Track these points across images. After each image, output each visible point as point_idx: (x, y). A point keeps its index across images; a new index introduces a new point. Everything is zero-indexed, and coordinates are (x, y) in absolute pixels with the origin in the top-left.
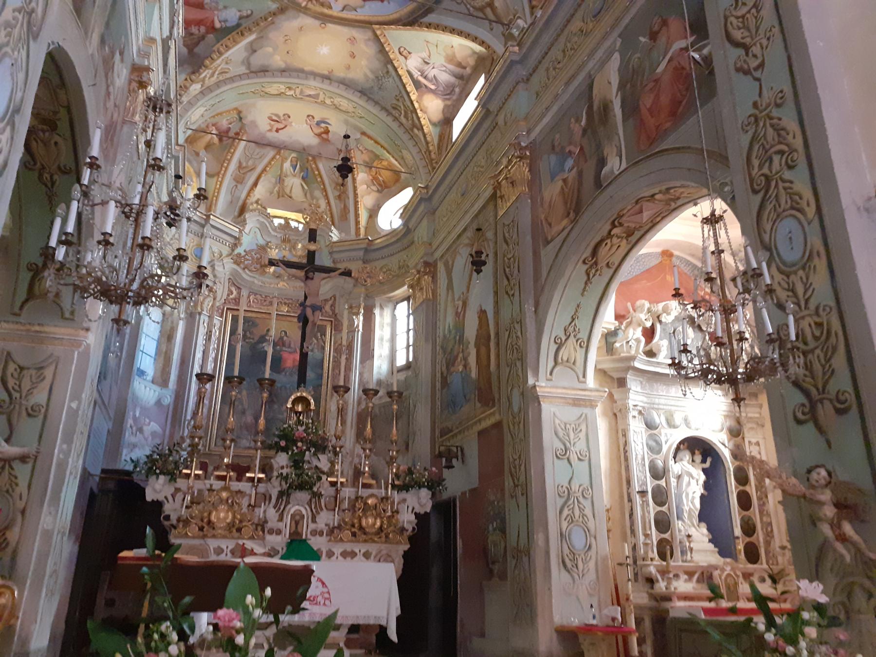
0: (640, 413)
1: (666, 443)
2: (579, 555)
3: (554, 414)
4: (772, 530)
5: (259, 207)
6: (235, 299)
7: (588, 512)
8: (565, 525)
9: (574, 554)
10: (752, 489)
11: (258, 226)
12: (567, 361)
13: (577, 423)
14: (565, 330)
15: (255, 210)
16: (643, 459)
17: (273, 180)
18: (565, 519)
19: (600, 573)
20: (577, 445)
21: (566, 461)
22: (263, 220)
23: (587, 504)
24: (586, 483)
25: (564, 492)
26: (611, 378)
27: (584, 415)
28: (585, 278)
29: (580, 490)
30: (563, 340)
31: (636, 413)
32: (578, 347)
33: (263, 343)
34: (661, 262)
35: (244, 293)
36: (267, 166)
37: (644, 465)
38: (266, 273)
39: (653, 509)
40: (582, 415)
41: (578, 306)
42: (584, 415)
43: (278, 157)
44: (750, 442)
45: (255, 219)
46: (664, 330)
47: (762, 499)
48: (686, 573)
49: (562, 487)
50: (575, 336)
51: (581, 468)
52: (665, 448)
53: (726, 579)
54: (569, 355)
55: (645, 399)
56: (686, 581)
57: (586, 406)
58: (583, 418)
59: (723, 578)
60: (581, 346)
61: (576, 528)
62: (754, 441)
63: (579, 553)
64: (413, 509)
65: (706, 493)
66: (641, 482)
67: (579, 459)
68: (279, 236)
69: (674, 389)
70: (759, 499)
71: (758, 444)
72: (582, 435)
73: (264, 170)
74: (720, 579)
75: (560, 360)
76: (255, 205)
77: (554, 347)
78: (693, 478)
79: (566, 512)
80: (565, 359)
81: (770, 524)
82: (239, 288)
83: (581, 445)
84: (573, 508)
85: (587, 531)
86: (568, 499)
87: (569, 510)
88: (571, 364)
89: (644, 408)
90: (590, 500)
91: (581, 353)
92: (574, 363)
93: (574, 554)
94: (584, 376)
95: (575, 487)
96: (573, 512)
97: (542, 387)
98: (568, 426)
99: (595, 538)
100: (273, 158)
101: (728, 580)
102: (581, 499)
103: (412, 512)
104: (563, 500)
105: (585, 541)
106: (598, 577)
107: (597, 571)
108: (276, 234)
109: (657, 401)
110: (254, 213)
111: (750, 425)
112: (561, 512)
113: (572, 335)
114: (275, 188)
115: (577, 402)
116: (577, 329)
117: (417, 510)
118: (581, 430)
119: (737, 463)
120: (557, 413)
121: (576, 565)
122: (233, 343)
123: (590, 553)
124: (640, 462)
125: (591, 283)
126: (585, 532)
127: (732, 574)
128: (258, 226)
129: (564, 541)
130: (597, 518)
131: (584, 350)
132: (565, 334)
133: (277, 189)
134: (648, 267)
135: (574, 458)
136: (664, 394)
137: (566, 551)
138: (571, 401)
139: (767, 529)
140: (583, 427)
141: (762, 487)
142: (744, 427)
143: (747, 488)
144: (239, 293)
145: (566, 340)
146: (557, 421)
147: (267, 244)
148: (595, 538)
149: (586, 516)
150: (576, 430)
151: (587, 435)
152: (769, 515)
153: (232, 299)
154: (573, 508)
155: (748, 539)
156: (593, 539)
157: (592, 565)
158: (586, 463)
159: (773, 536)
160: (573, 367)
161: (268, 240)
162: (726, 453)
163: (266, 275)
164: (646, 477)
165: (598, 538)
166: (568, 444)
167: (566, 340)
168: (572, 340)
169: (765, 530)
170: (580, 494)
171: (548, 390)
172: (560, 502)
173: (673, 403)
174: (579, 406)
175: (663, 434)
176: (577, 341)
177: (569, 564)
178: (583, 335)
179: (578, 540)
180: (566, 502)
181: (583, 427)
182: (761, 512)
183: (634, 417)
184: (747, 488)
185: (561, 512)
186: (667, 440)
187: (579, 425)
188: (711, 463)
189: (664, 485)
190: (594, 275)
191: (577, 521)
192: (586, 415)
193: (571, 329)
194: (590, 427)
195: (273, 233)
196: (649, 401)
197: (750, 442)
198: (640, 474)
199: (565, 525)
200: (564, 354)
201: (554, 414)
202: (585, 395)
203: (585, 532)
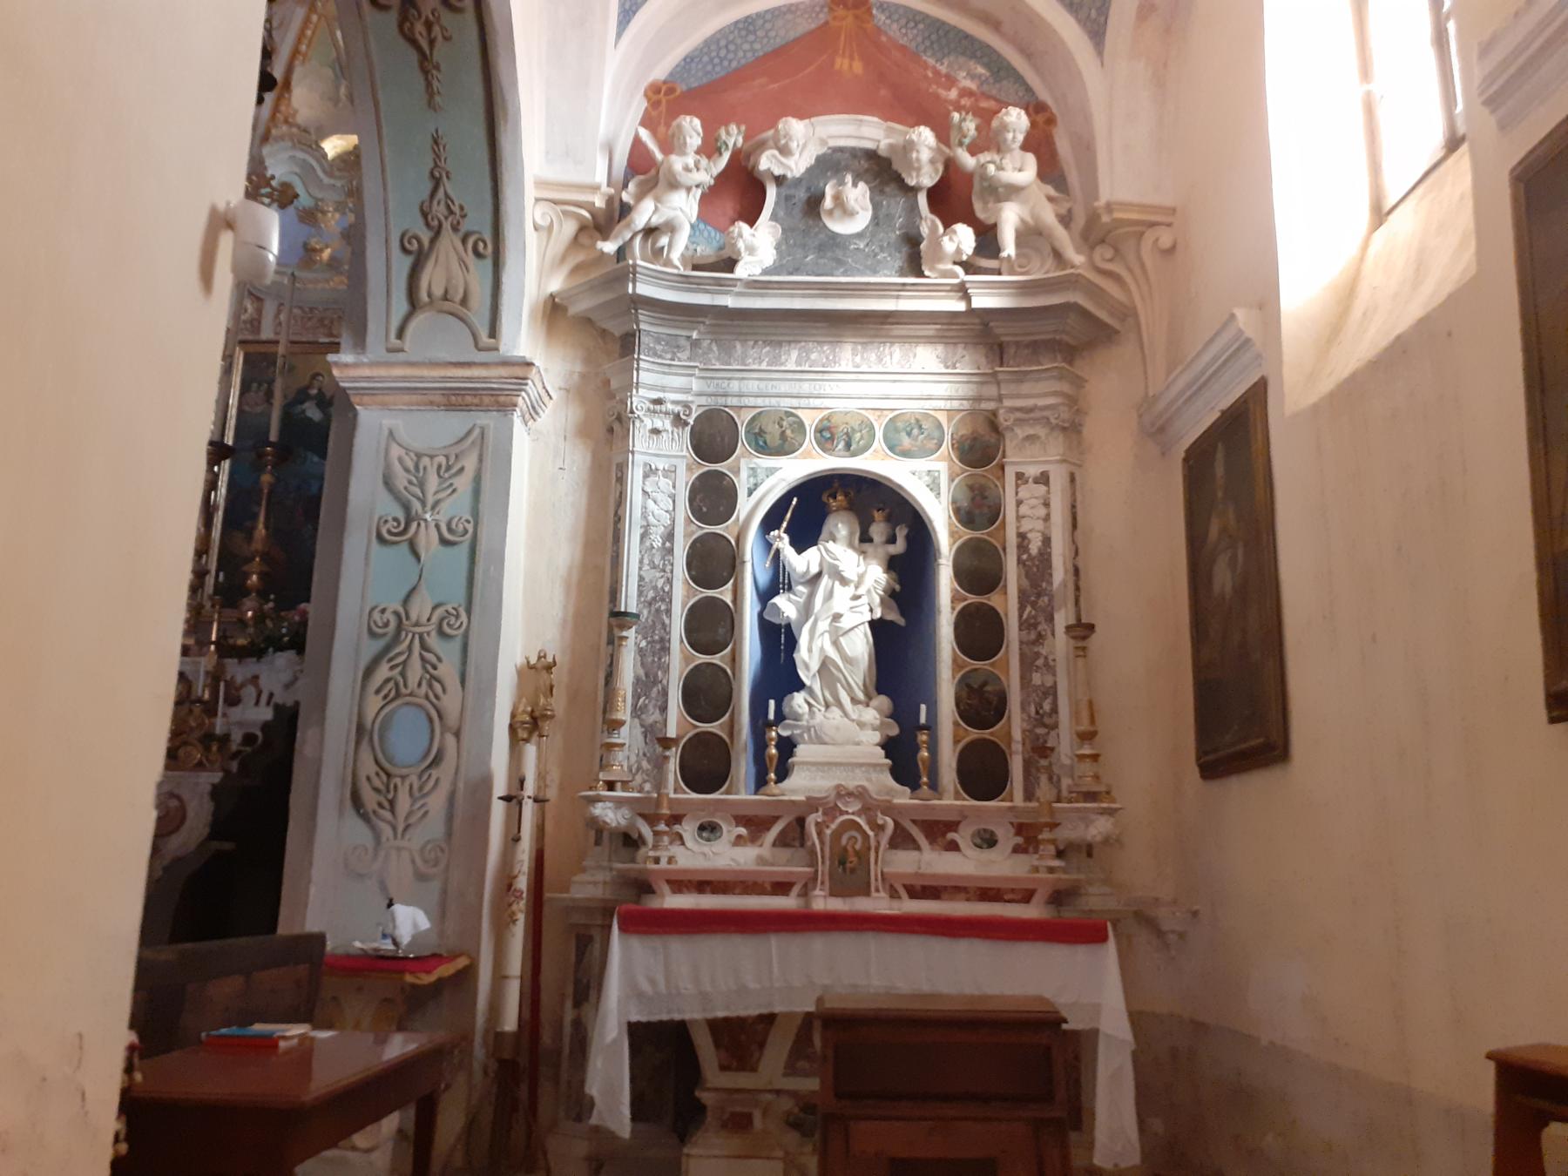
0: (678, 421)
1: (750, 493)
2: (403, 778)
3: (391, 433)
4: (1055, 710)
5: (294, 130)
6: (251, 321)
7: (448, 670)
8: (374, 703)
9: (389, 775)
10: (1007, 602)
11: (297, 170)
12: (445, 298)
13: (453, 452)
14: (425, 215)
15: (282, 138)
16: (670, 536)
17: (329, 72)
18: (378, 692)
19: (457, 822)
20: (444, 506)
21: (405, 548)
22: (300, 155)
23: (448, 653)
24: (457, 598)
25: (386, 625)
26: (604, 333)
27: (477, 432)
28: (413, 57)
29: (435, 619)
30: (426, 243)
31: (665, 423)
32: (470, 258)
33: (302, 403)
34: (826, 23)
35: (269, 308)
36: (299, 40)
37: (671, 551)
38: (315, 262)
39: (679, 660)
40: (469, 433)
41: (436, 142)
42: (477, 432)
43: (315, 18)
44: (1020, 476)
45: (285, 155)
46: (788, 198)
47: (1035, 626)
48: (742, 820)
49: (383, 611)
50: (455, 229)
51: (447, 569)
52: (744, 505)
53: (837, 835)
54: (449, 280)
55: (696, 385)
56: (739, 841)
57: (480, 407)
58: (470, 440)
59: (828, 832)
60: (478, 254)
61: (405, 709)
62: (1032, 471)
63: (404, 771)
64: (271, 695)
65: (894, 616)
66: (651, 594)
67: (444, 542)
68: (339, 184)
69: (794, 354)
70: (1026, 625)
71: (1043, 479)
72: (463, 483)
73: (295, 53)
74: (820, 834)
75: (424, 296)
76: (285, 128)
77: (402, 264)
78: (857, 587)
79: (383, 672)
80: (438, 291)
81: (1052, 691)
82: (259, 299)
83: (455, 507)
84: (404, 663)
85: (435, 717)
86: (396, 639)
87: (392, 668)
88: (454, 305)
89: (686, 405)
90: (456, 645)
91: (479, 276)
92: (464, 302)
93: (389, 775)
94: (493, 332)
95: (421, 608)
96: (403, 674)
97: (346, 365)
98: (425, 461)
99: (457, 735)
100: (307, 21)
101: (844, 841)
102: (433, 641)
103: (268, 703)
104: (379, 645)
105: (426, 743)
106: (449, 834)
107: (450, 818)
108: (332, 181)
109: (735, 386)
110: (282, 144)
111: (1020, 432)
112: (369, 672)
113: (447, 225)
114: (337, 88)
115: (456, 399)
116: (456, 209)
117: (278, 699)
118: (462, 469)
119: (968, 534)
120: (402, 434)
121: (392, 803)
122: (247, 408)
123: (435, 773)
124: (658, 543)
125: (437, 68)
126: (431, 720)
127: (861, 821)
128: (297, 170)
129: (365, 745)
130: (470, 683)
131: (488, 263)
132: (428, 225)
133: (343, 90)
134: (779, 42)
135: (428, 541)
136: (764, 366)
137: (368, 767)
138: (438, 398)
139: (1039, 706)
140: (470, 463)
141: (1039, 595)
142: (1008, 435)
143: (994, 600)
144: (259, 311)
145: (433, 241)
146: (396, 451)
147: (317, 205)
148: (457, 735)
149: (438, 681)
150: (448, 468)
151: (478, 480)
152: (1050, 668)
153: (245, 322)
154: (404, 663)
155: (974, 734)
156: (450, 740)
157: (436, 803)
158: (462, 551)
159: (1055, 726)
160: (462, 311)
161: (320, 196)
162: (939, 514)
163: (317, 266)
164: (670, 581)
165: (465, 736)
166: (416, 505)
167: (433, 241)
168: (449, 241)
169: (1032, 710)
170: (432, 627)
171: (367, 372)
172: (371, 648)
173: (784, 387)
174: (465, 407)
175: (744, 474)
176: (464, 241)
177: (370, 799)
178: (478, 221)
179: (407, 740)
180: (387, 649)
181: (470, 463)
182: (1028, 663)
183: (656, 431)
184: (994, 600)
185: (369, 672)
186: (756, 486)
187: (457, 456)
188: (908, 538)
189: (728, 599)
190: (432, 42)
191: (411, 695)
192: (482, 435)
193: (439, 210)
194: (488, 463)
195: (326, 180)
196: (711, 390)
197: (1020, 476)
198: (649, 574)
199: (374, 703)
200: (433, 278)
201: (391, 433)
202: (470, 379)
203: (431, 720)
